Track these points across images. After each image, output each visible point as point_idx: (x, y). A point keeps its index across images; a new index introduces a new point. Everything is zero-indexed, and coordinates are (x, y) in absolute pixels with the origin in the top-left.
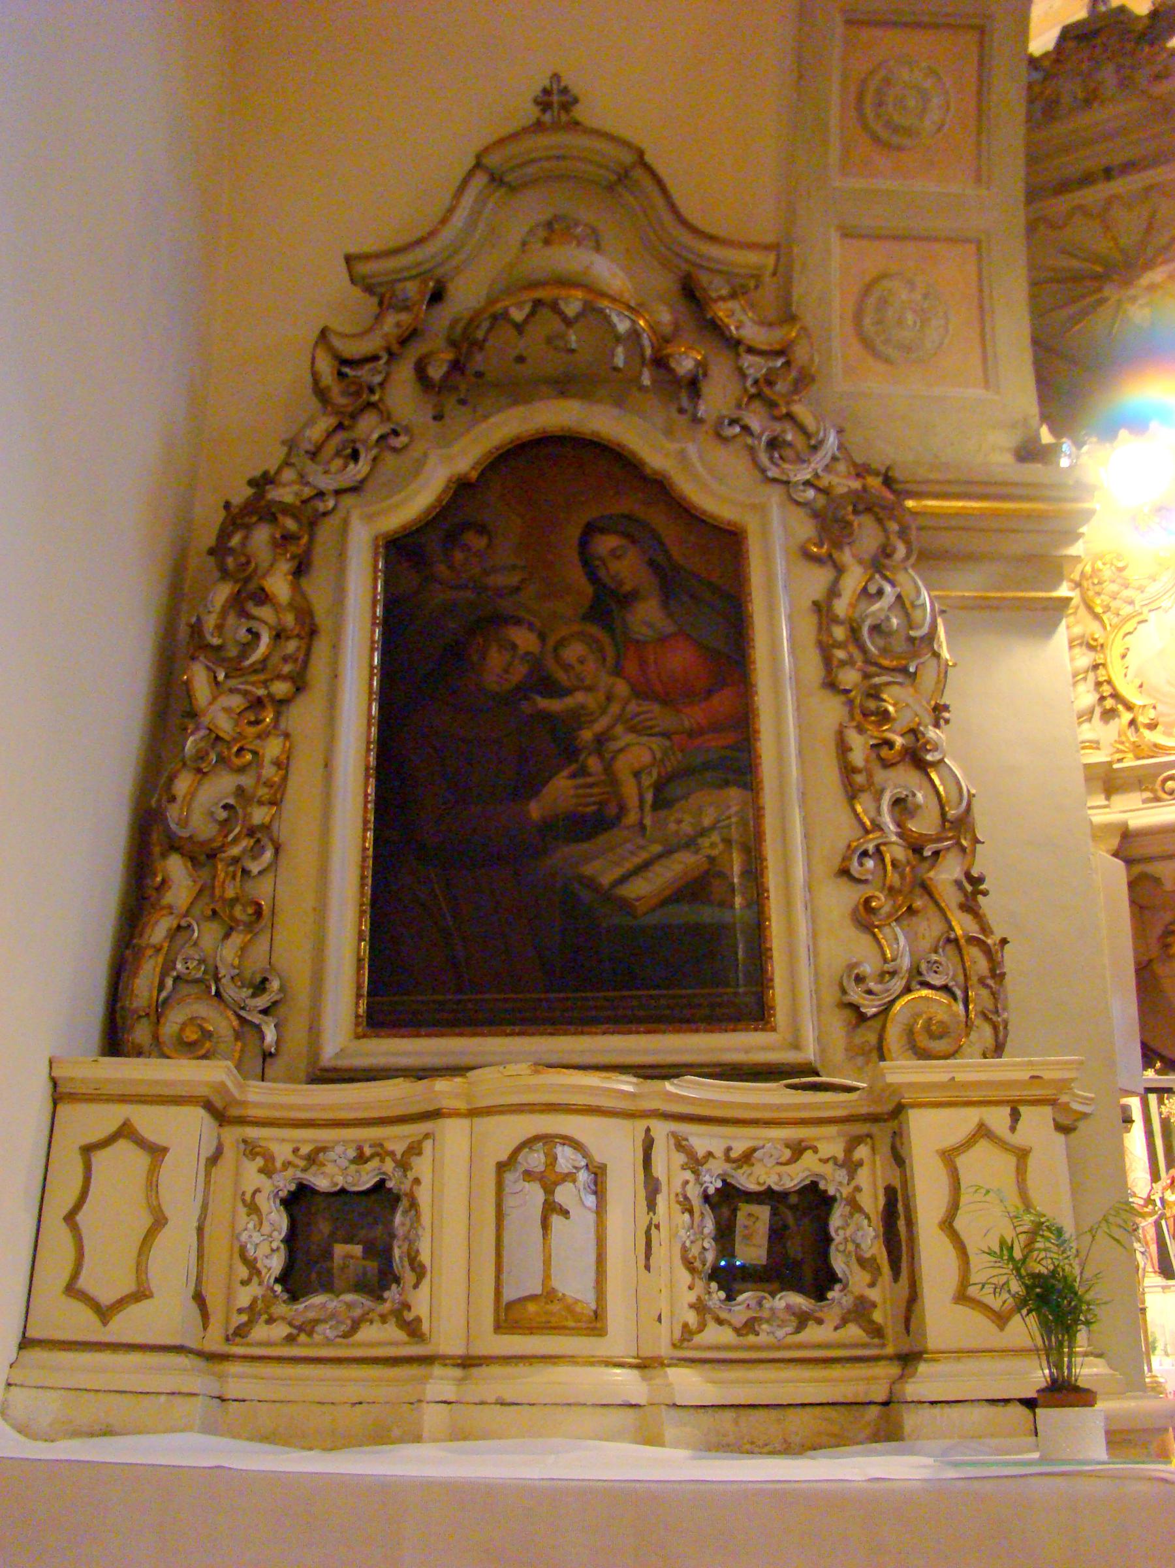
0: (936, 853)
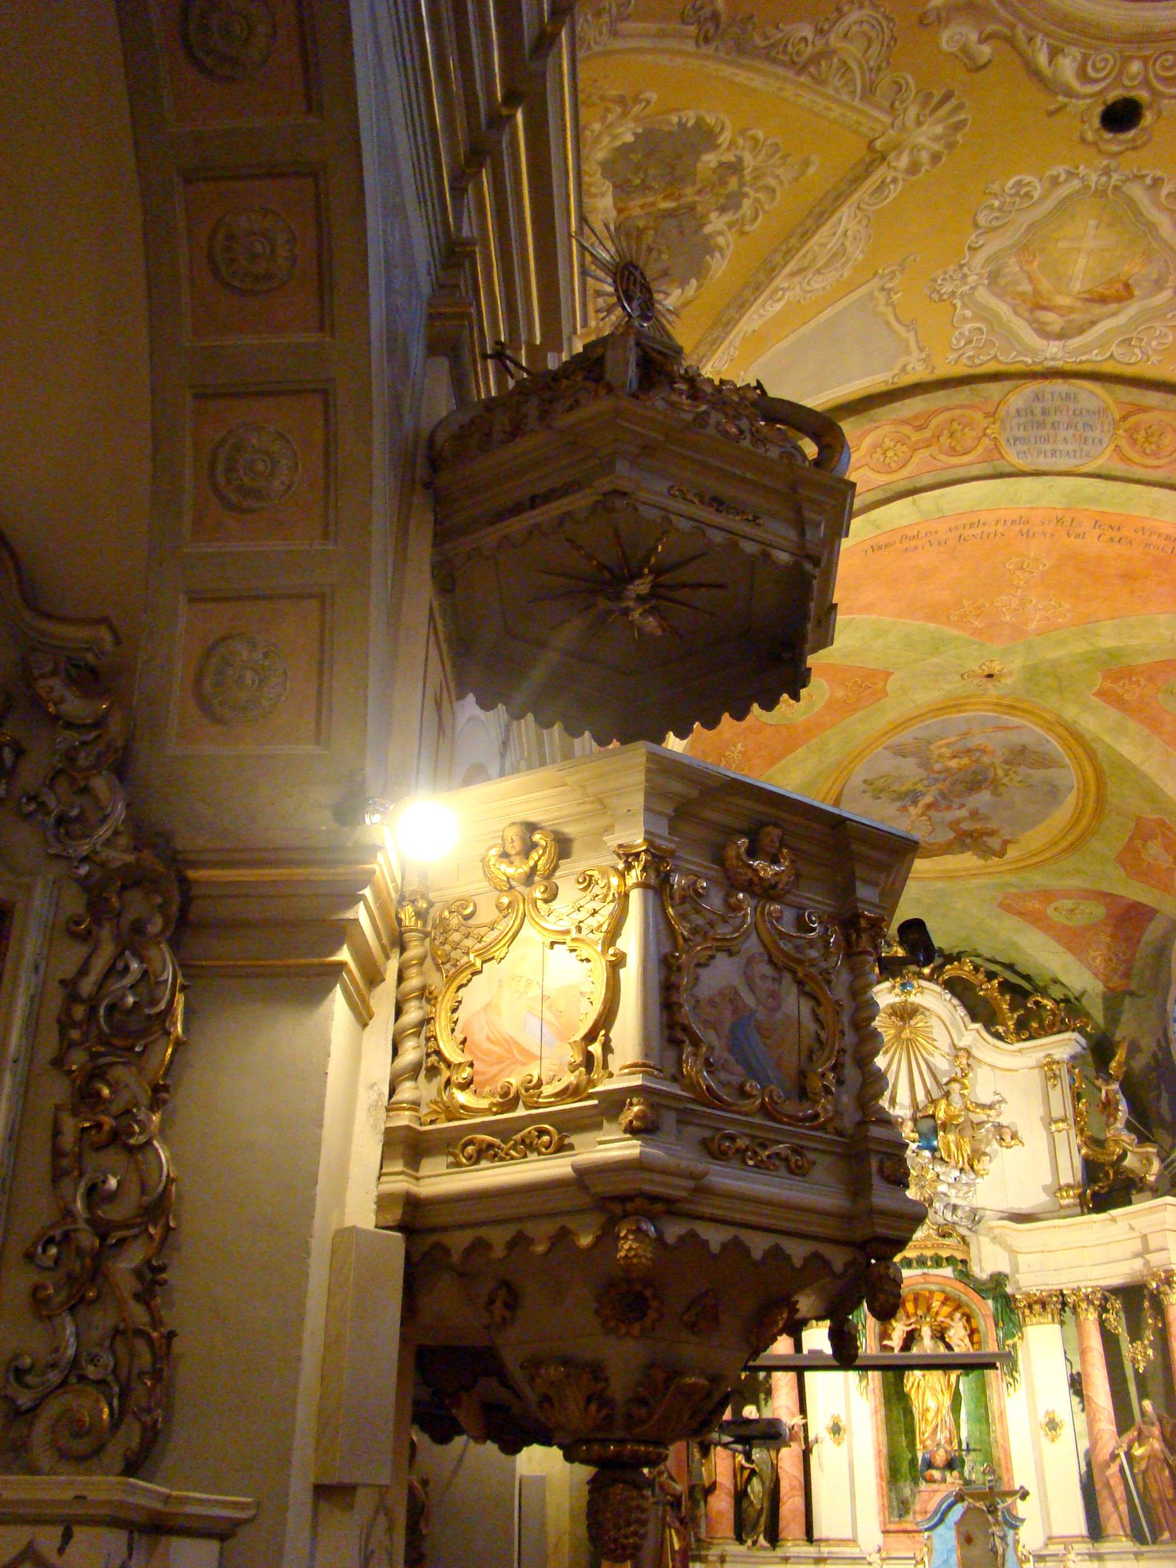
0: (122, 1241)
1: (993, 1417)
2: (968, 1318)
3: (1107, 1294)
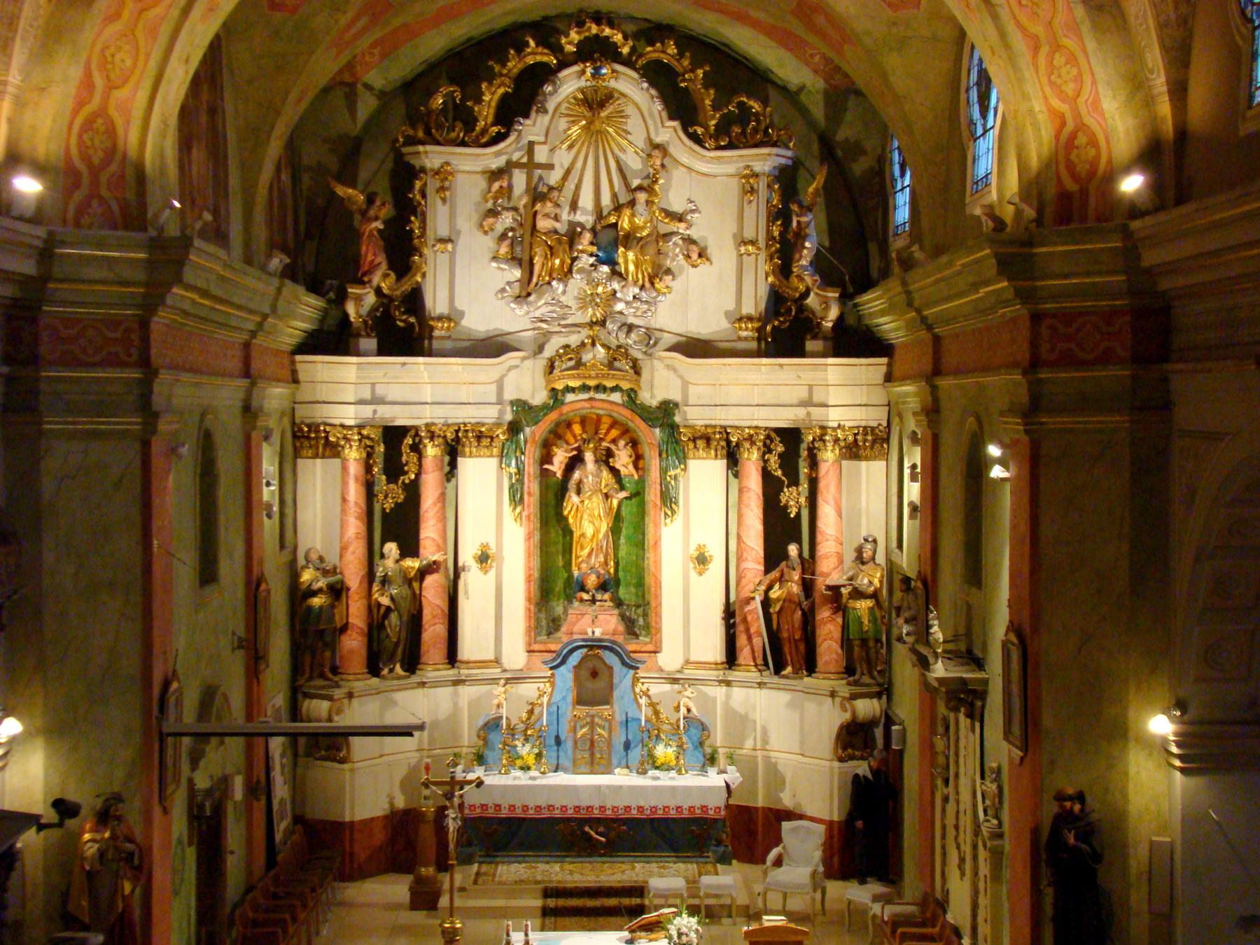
2: (634, 443)
3: (773, 435)
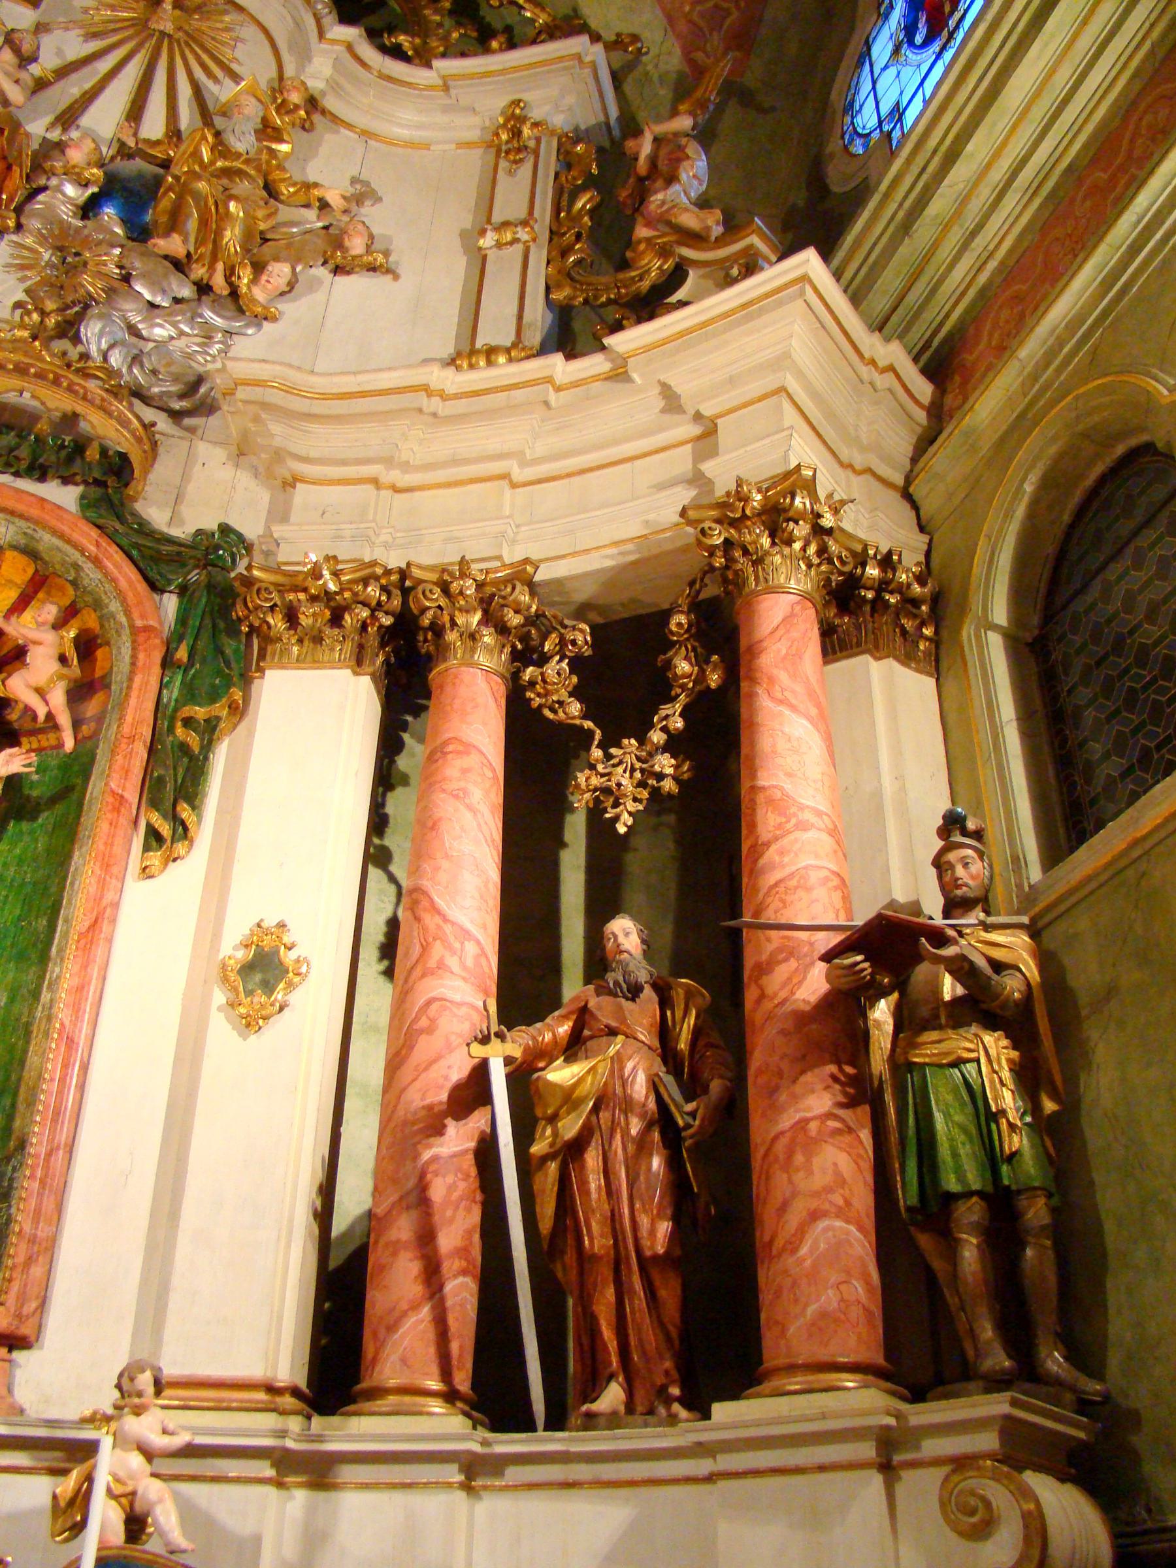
1: (66, 935)
